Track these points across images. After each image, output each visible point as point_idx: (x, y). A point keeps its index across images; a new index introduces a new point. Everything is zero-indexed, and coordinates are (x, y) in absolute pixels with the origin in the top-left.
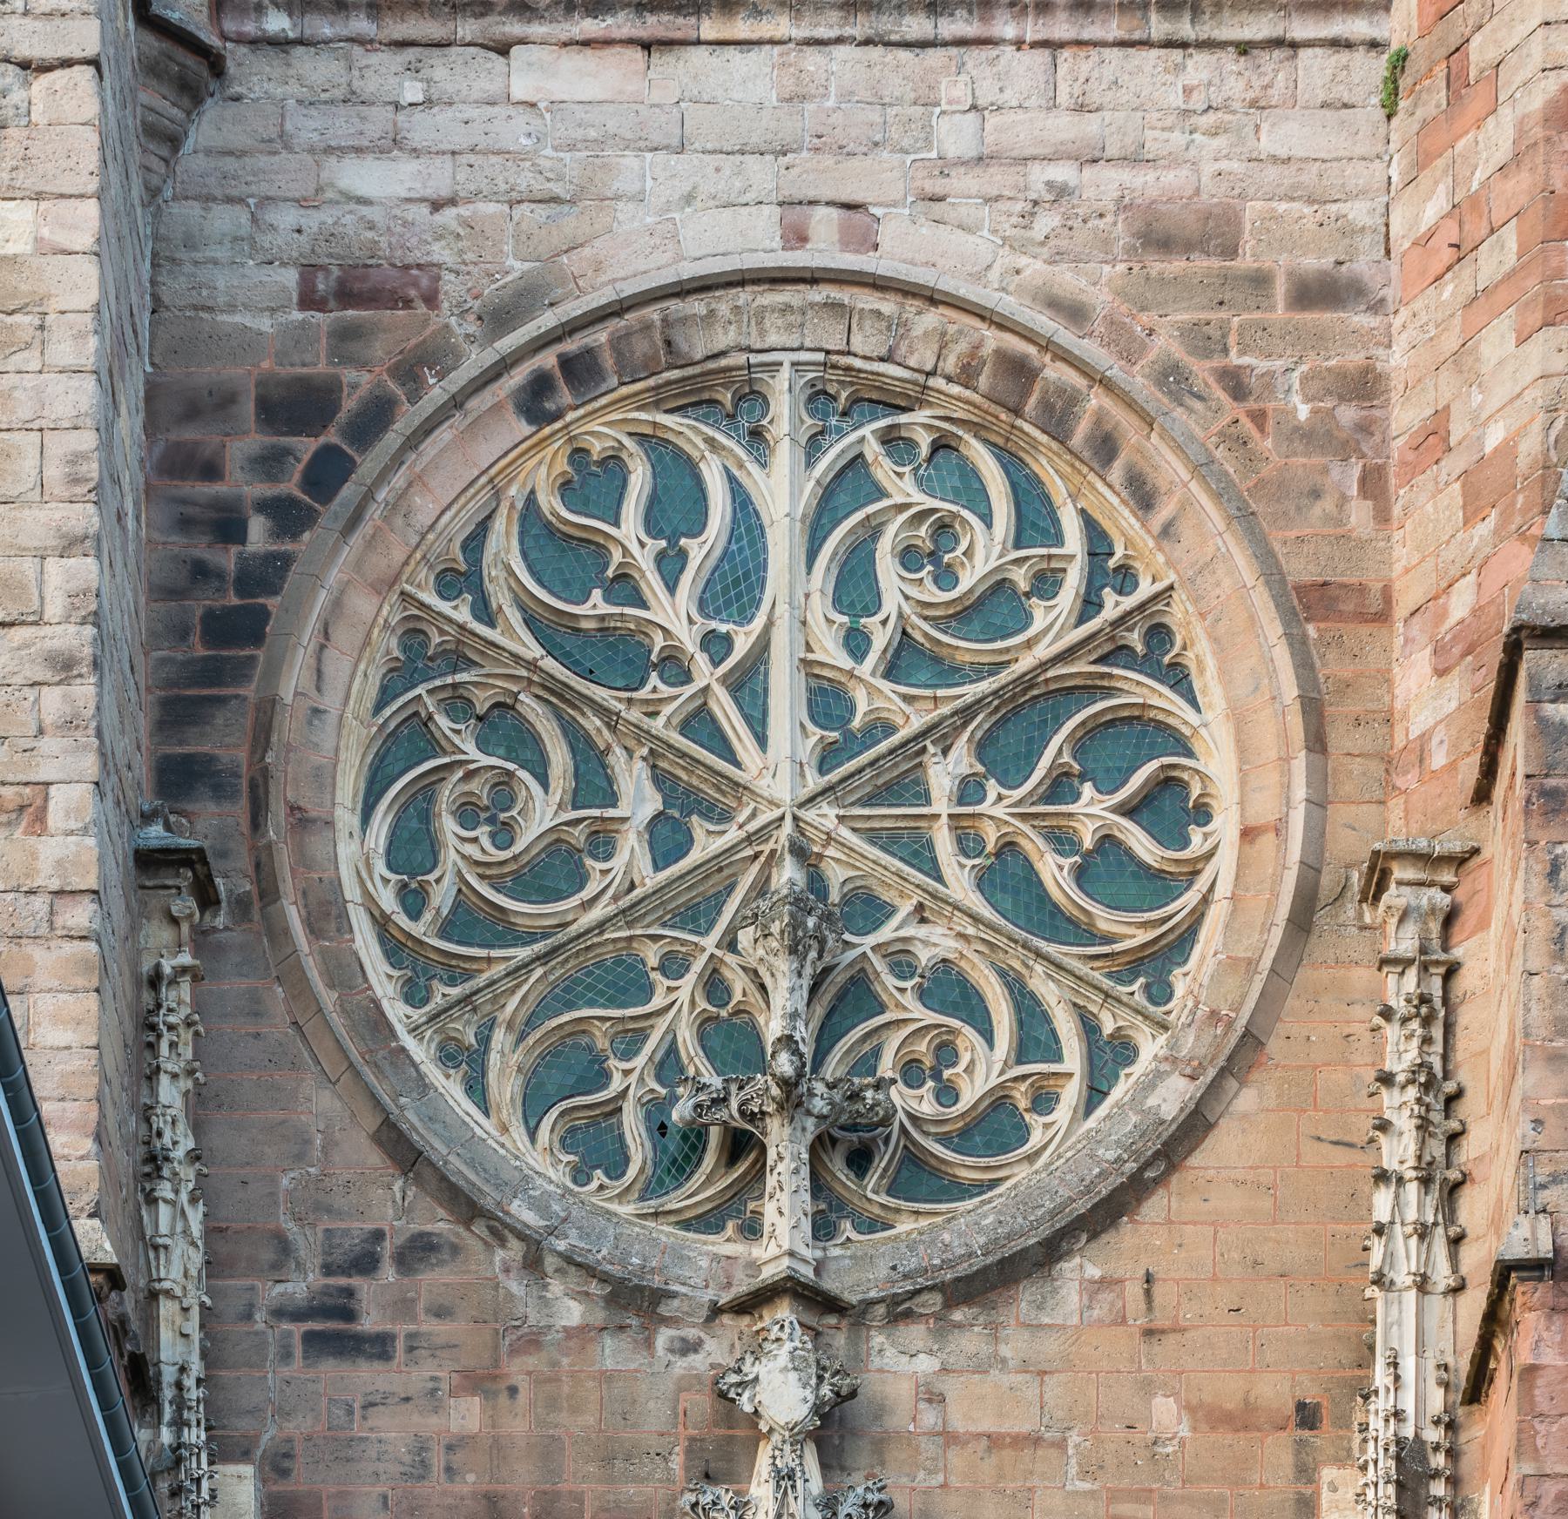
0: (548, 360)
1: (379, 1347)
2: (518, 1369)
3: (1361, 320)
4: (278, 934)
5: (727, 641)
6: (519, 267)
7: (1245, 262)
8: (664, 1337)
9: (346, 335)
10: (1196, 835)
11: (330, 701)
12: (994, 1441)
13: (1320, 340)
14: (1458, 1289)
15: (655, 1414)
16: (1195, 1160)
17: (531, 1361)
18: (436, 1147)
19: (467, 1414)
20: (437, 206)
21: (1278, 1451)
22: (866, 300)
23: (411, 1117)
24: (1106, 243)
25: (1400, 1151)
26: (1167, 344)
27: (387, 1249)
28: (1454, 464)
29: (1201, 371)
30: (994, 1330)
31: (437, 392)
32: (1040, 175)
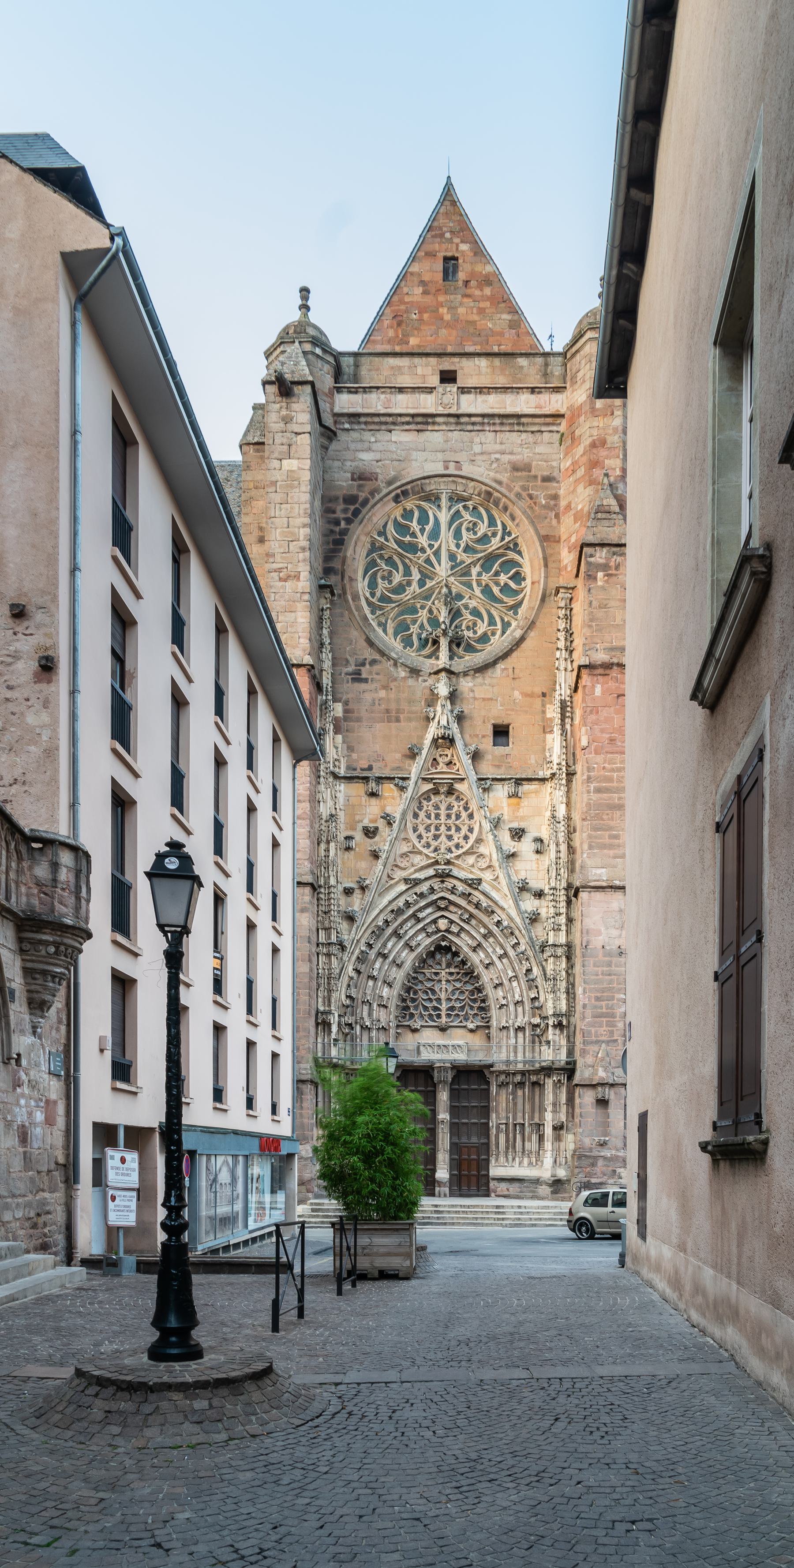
0: (399, 491)
1: (366, 680)
2: (392, 685)
3: (555, 484)
4: (347, 601)
5: (433, 545)
6: (393, 473)
7: (533, 473)
8: (420, 679)
9: (360, 486)
10: (523, 583)
11: (357, 557)
12: (484, 699)
13: (547, 488)
14: (572, 671)
15: (419, 694)
16: (522, 645)
17: (395, 683)
18: (377, 642)
19: (382, 694)
20: (377, 461)
21: (538, 702)
22: (460, 480)
23: (372, 637)
24: (506, 470)
25: (561, 644)
26: (517, 489)
27: (367, 662)
28: (572, 512)
29: (524, 494)
30: (484, 678)
31: (377, 497)
32: (493, 456)
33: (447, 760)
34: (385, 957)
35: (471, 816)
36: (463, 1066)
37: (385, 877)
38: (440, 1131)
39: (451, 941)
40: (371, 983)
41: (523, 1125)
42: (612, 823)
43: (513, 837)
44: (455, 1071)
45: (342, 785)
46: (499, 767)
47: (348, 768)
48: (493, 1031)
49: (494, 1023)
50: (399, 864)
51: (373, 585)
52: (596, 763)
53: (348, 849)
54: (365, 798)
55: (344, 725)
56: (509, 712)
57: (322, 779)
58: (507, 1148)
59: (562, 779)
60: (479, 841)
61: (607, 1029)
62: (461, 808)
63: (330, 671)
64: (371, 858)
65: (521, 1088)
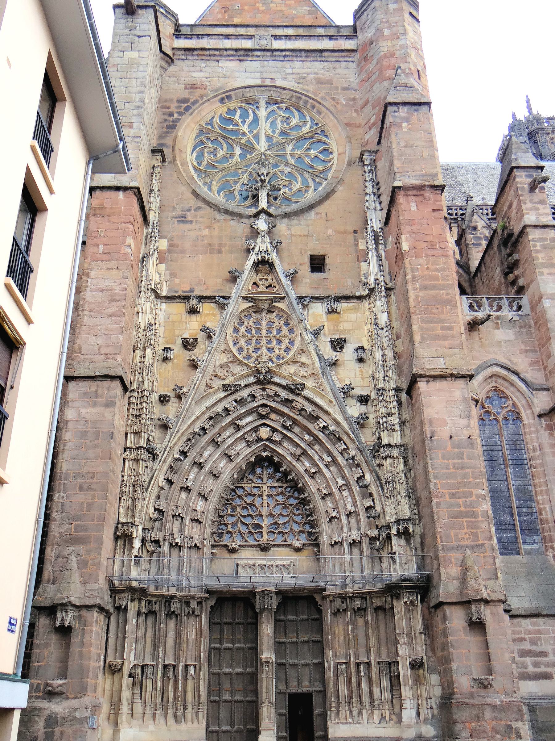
0: (224, 95)
1: (191, 222)
12: (300, 236)
14: (381, 210)
17: (218, 224)
18: (202, 194)
19: (206, 232)
20: (207, 78)
21: (351, 237)
23: (198, 191)
25: (369, 190)
26: (322, 94)
27: (193, 209)
33: (267, 283)
34: (200, 466)
35: (291, 331)
36: (290, 591)
37: (203, 386)
38: (264, 675)
39: (274, 451)
40: (184, 495)
41: (368, 664)
42: (442, 316)
43: (334, 348)
44: (281, 597)
45: (163, 304)
46: (316, 288)
47: (170, 290)
48: (325, 548)
49: (325, 539)
50: (219, 374)
51: (200, 158)
52: (420, 265)
53: (166, 359)
54: (185, 316)
55: (168, 256)
56: (324, 246)
57: (142, 293)
58: (350, 697)
59: (381, 292)
60: (301, 351)
61: (469, 531)
62: (282, 324)
63: (157, 211)
64: (190, 369)
65: (361, 616)
